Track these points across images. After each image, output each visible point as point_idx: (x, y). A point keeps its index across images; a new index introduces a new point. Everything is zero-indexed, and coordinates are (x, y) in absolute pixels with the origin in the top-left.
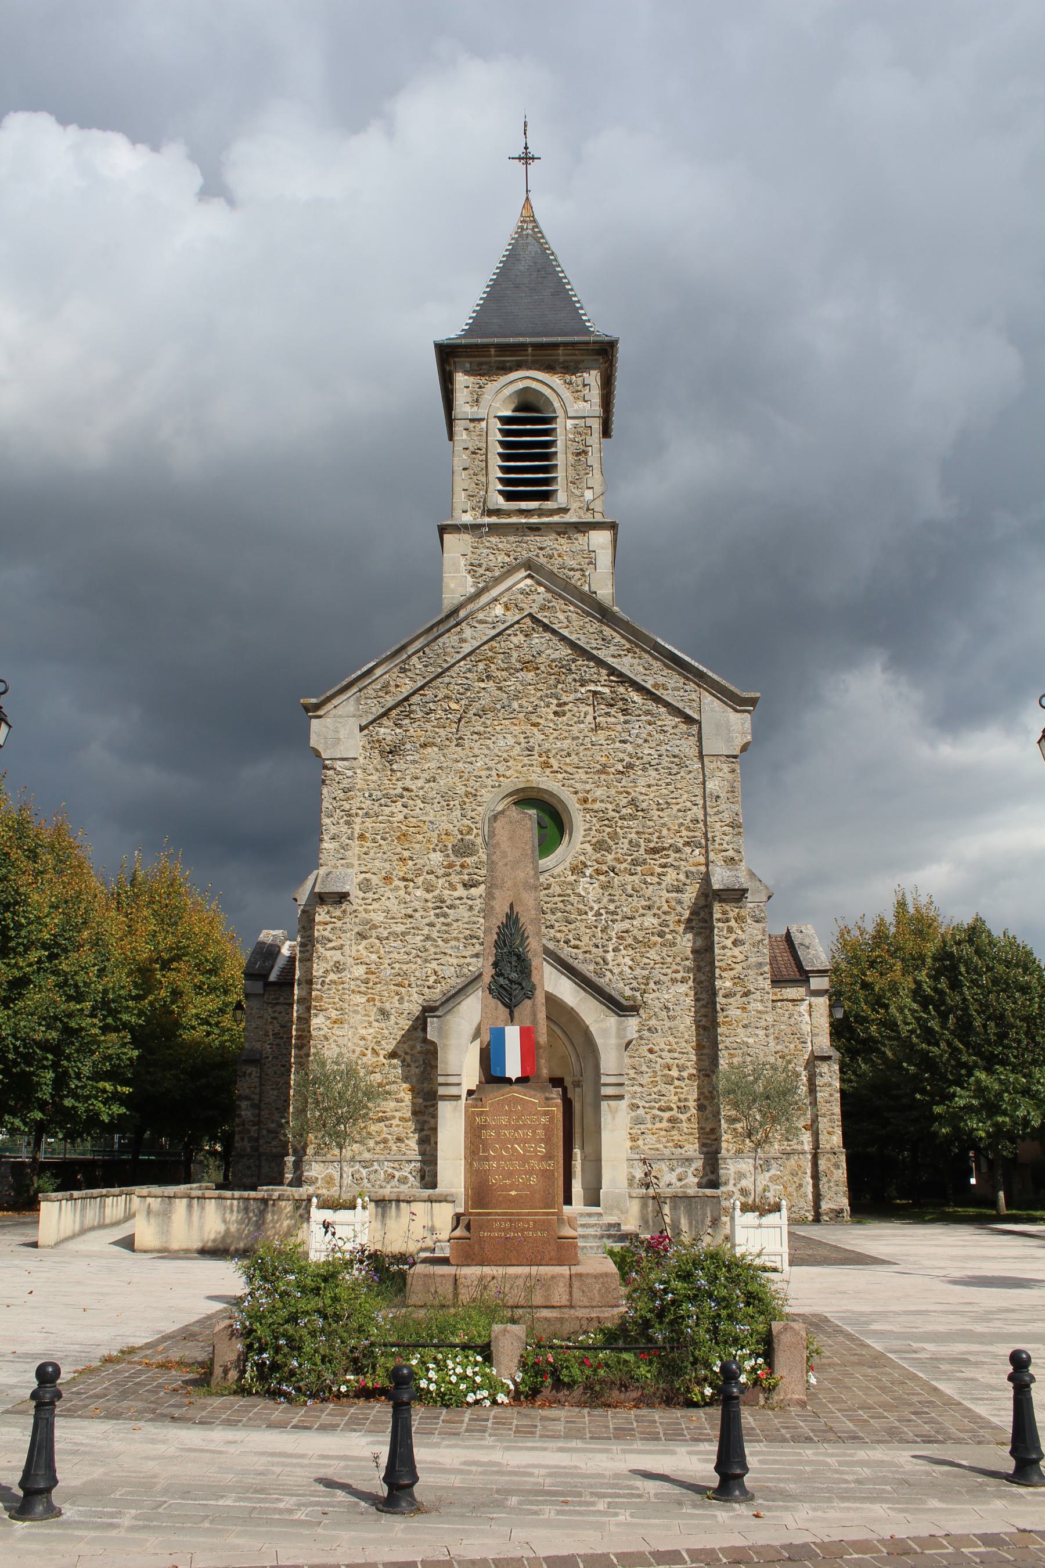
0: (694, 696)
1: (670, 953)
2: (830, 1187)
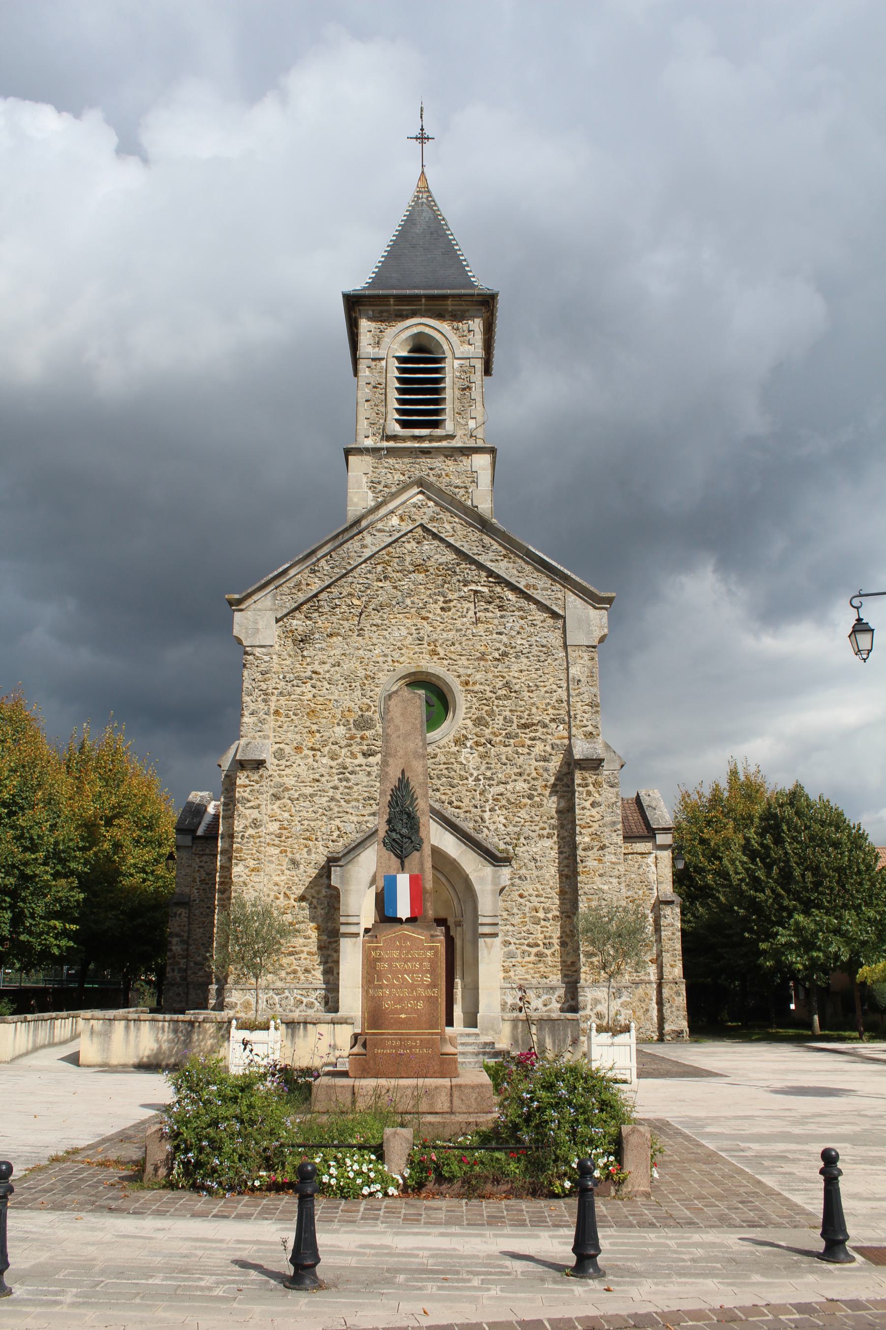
0: (559, 595)
2: (672, 1012)
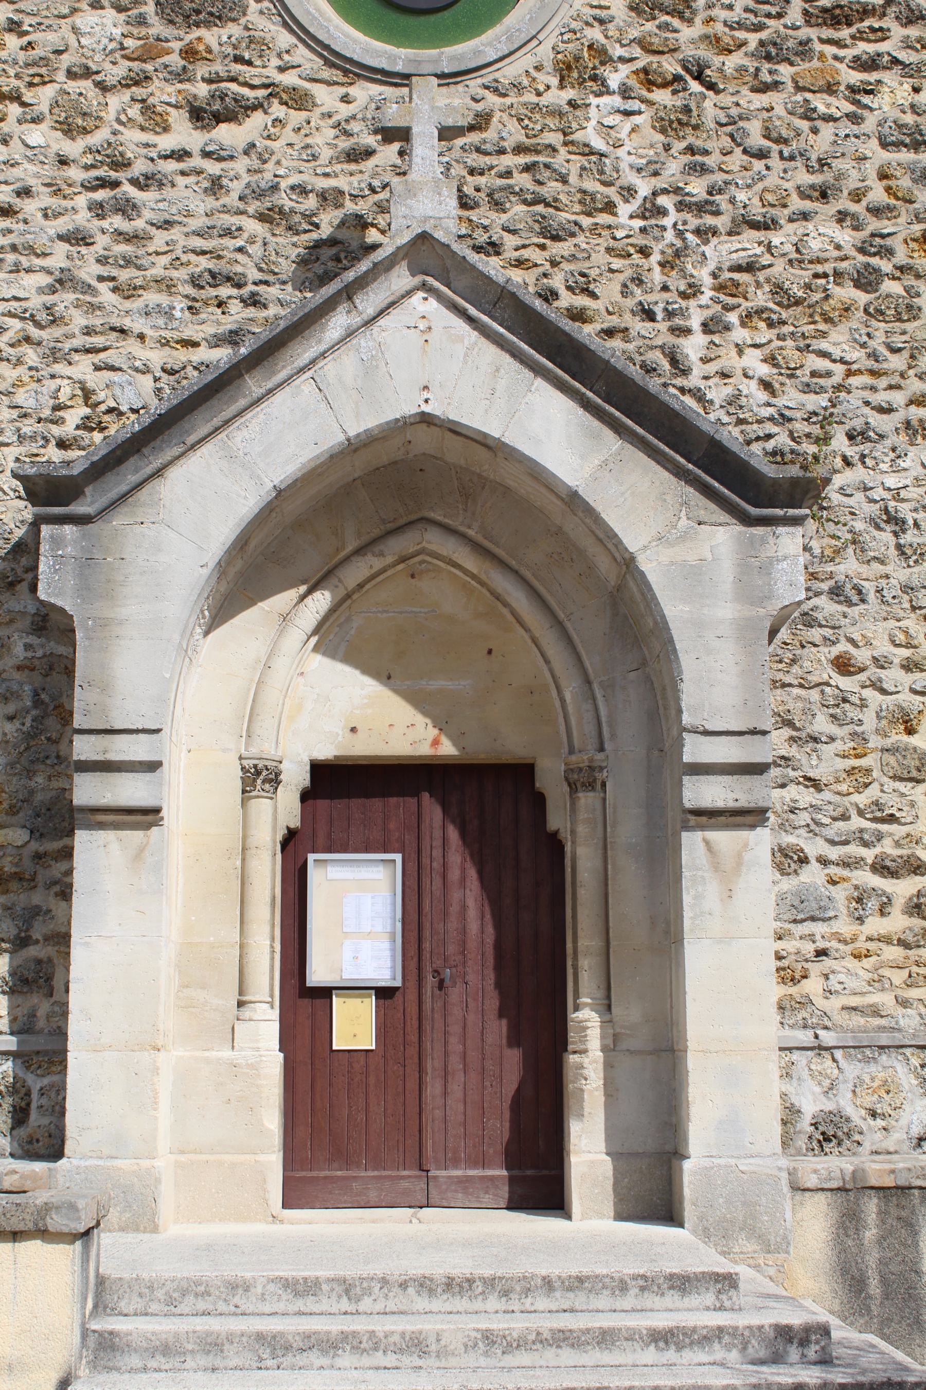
1: (898, 341)
